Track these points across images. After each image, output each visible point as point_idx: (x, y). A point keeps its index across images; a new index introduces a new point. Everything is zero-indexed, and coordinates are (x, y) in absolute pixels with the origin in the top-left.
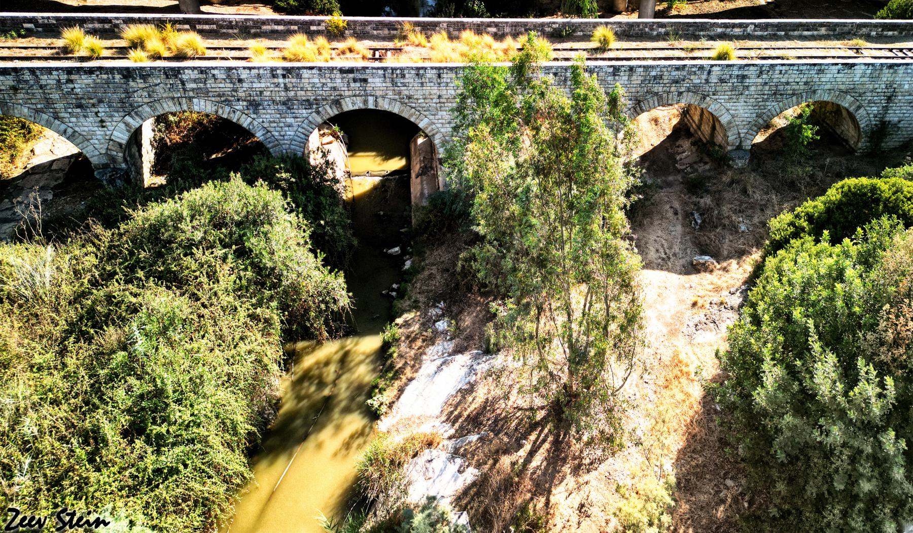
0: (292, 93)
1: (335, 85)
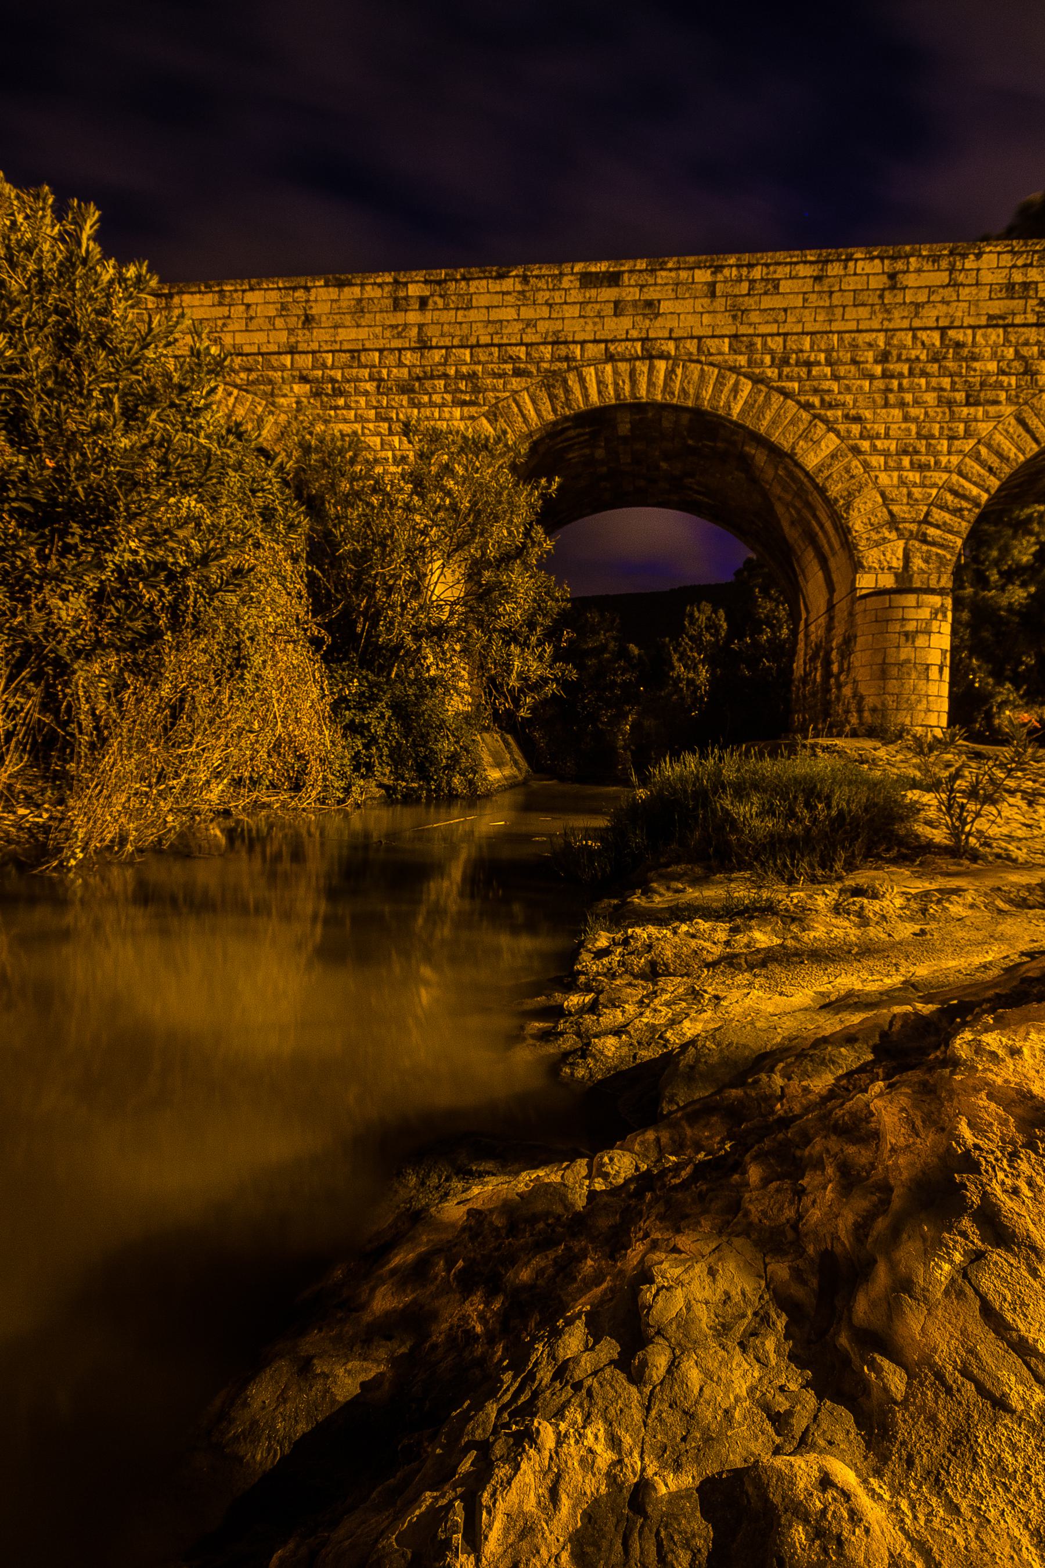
1: (558, 325)
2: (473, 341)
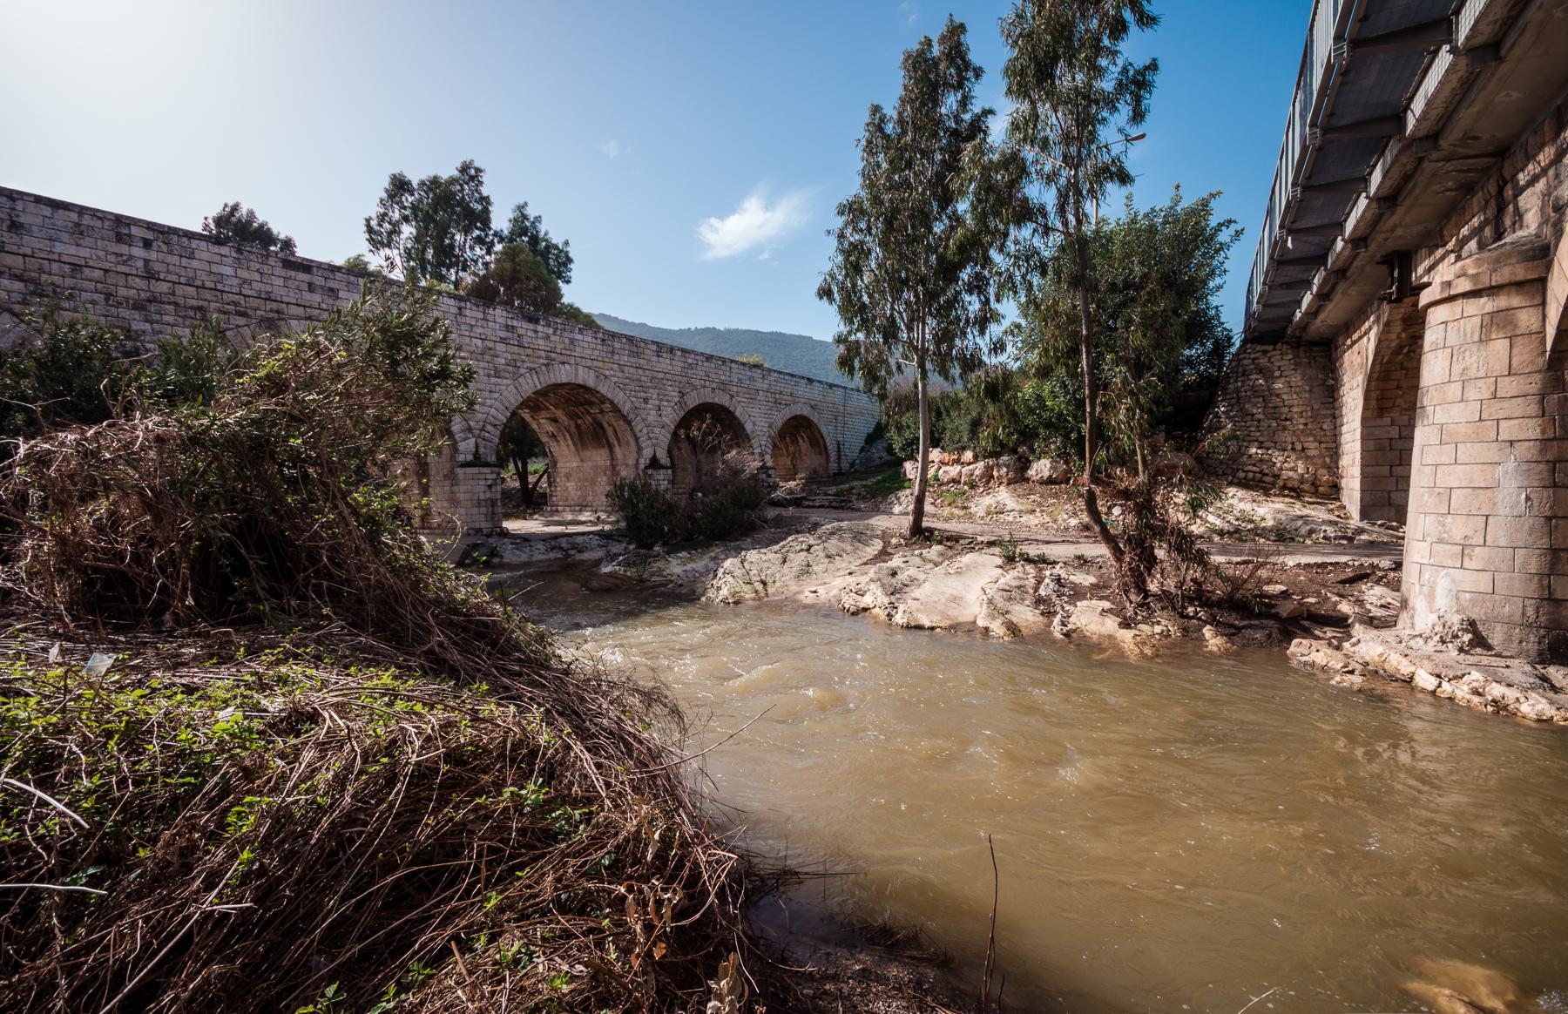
0: (164, 287)
1: (268, 288)
2: (198, 283)
